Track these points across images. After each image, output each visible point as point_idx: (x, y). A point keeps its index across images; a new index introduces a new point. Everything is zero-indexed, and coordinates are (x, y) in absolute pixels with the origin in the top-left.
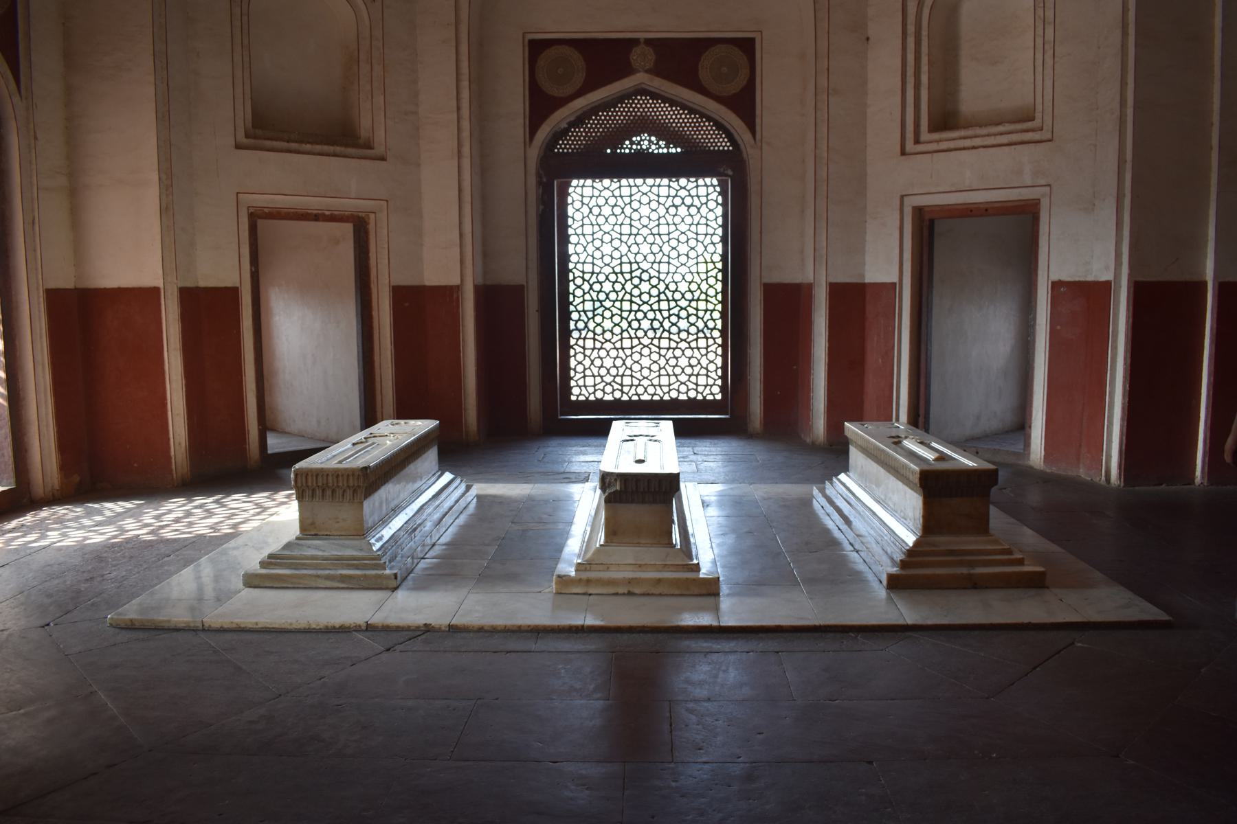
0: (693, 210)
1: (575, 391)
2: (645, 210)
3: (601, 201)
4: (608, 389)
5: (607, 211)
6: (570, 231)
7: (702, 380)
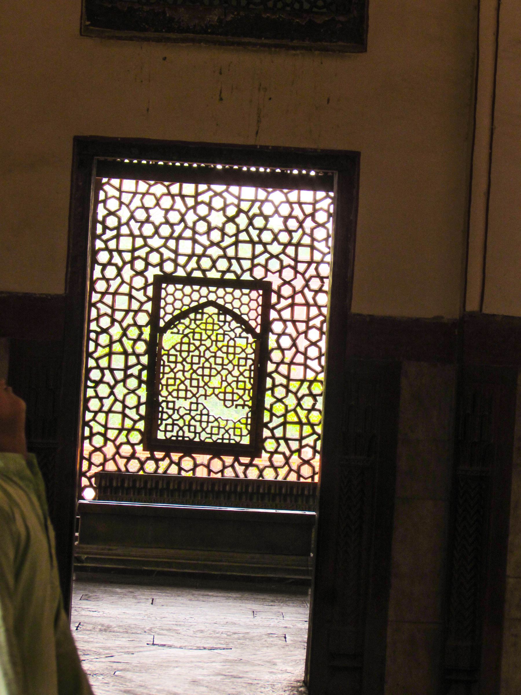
0: (292, 224)
2: (217, 219)
3: (149, 201)
5: (157, 216)
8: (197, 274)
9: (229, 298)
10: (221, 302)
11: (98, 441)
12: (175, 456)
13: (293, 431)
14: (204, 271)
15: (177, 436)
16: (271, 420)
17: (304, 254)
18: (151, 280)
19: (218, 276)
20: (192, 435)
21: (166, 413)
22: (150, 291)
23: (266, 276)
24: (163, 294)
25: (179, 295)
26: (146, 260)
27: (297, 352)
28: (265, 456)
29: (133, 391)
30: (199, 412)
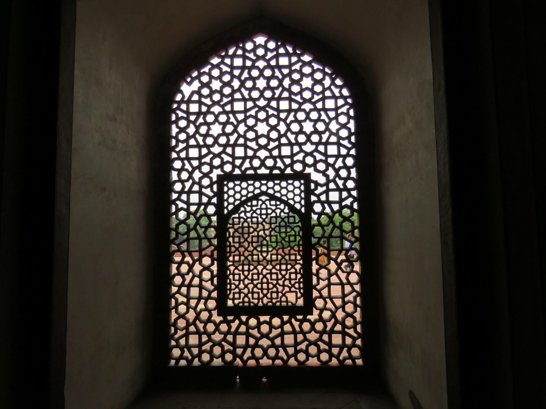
1: (176, 352)
4: (217, 350)
6: (174, 155)
7: (337, 339)
8: (251, 172)
9: (277, 188)
10: (271, 191)
11: (182, 309)
12: (244, 318)
13: (336, 291)
14: (255, 169)
15: (243, 302)
16: (318, 283)
17: (332, 150)
18: (215, 179)
19: (267, 172)
20: (256, 301)
21: (234, 284)
22: (215, 187)
23: (304, 169)
24: (226, 189)
25: (238, 189)
26: (211, 164)
27: (335, 227)
28: (316, 312)
29: (207, 268)
30: (260, 281)
